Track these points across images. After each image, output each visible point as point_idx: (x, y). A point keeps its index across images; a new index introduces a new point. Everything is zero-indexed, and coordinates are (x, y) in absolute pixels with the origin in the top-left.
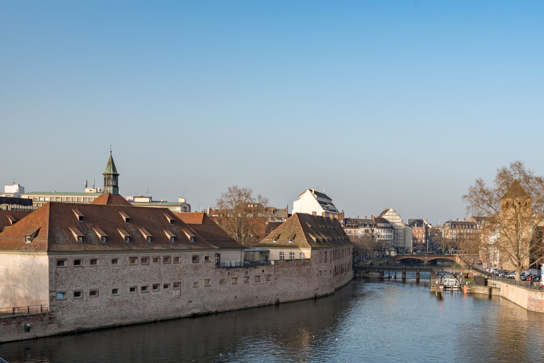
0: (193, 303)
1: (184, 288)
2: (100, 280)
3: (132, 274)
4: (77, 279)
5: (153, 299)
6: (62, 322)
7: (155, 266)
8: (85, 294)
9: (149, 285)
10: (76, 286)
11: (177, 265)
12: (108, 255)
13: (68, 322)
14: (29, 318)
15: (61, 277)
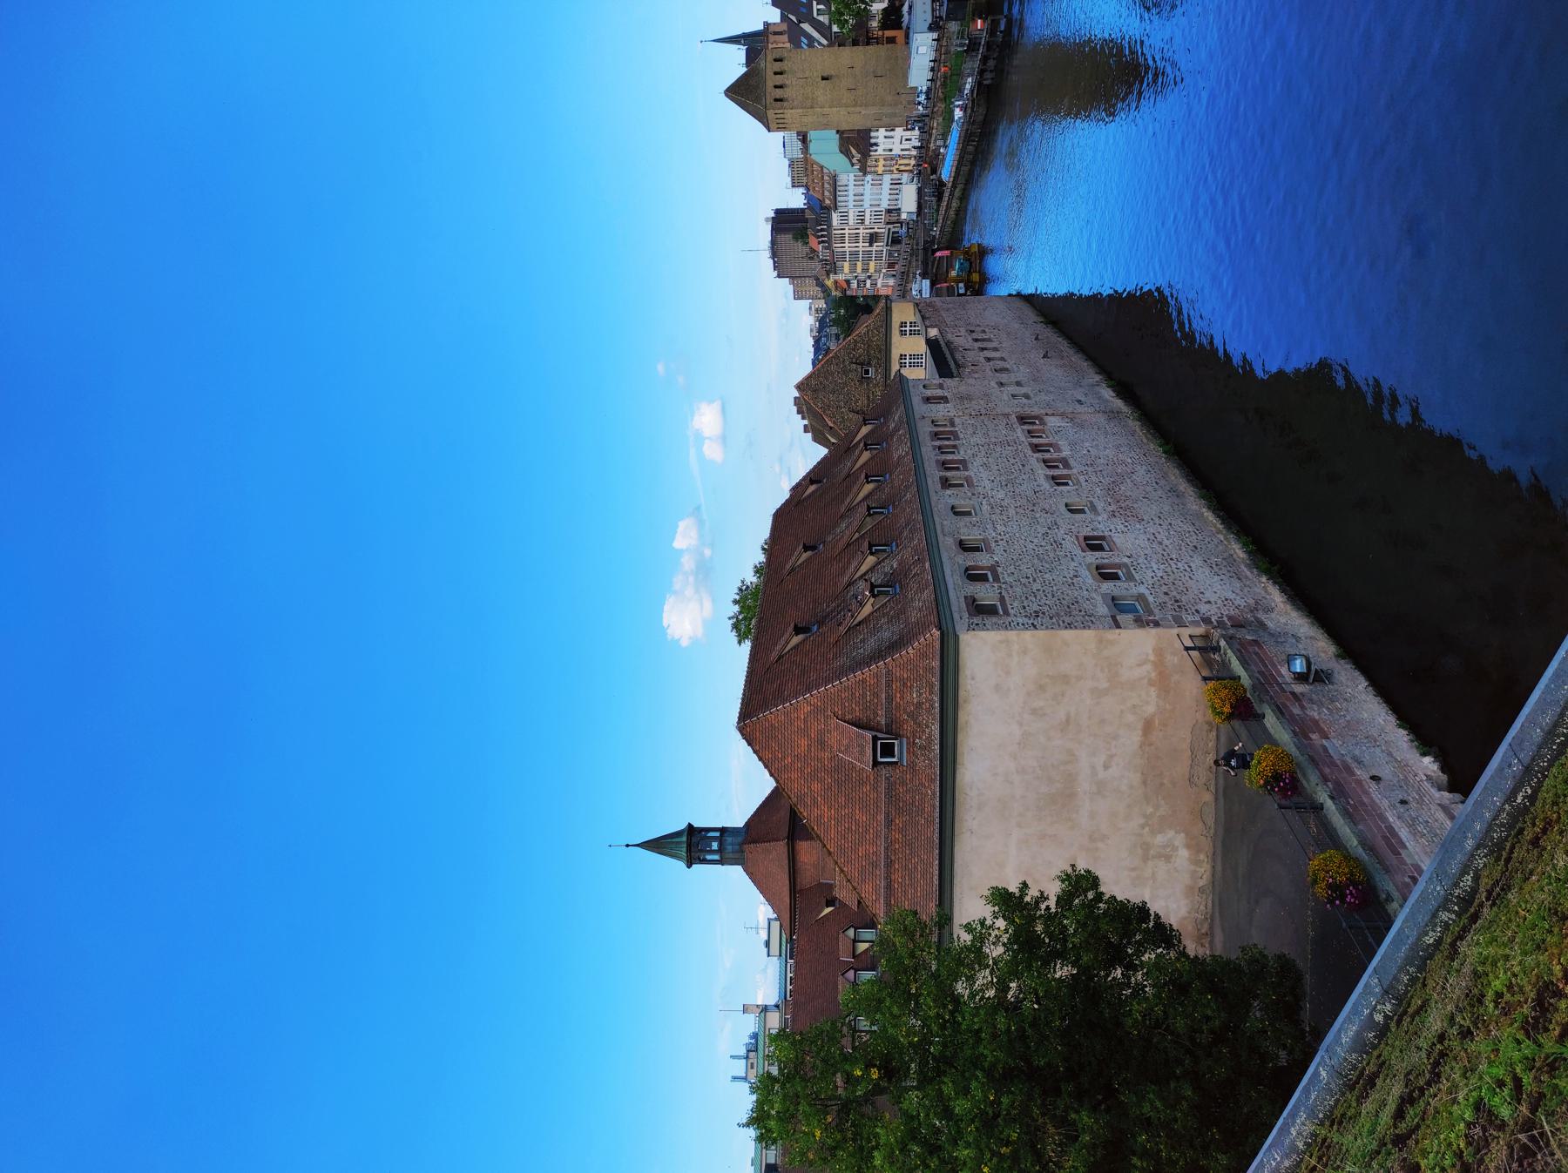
0: (1083, 399)
1: (1036, 411)
2: (1039, 535)
3: (1004, 483)
4: (1046, 576)
7: (969, 451)
8: (1106, 561)
9: (1037, 459)
10: (1076, 576)
11: (957, 421)
12: (942, 525)
13: (1238, 591)
14: (1260, 672)
15: (1047, 608)
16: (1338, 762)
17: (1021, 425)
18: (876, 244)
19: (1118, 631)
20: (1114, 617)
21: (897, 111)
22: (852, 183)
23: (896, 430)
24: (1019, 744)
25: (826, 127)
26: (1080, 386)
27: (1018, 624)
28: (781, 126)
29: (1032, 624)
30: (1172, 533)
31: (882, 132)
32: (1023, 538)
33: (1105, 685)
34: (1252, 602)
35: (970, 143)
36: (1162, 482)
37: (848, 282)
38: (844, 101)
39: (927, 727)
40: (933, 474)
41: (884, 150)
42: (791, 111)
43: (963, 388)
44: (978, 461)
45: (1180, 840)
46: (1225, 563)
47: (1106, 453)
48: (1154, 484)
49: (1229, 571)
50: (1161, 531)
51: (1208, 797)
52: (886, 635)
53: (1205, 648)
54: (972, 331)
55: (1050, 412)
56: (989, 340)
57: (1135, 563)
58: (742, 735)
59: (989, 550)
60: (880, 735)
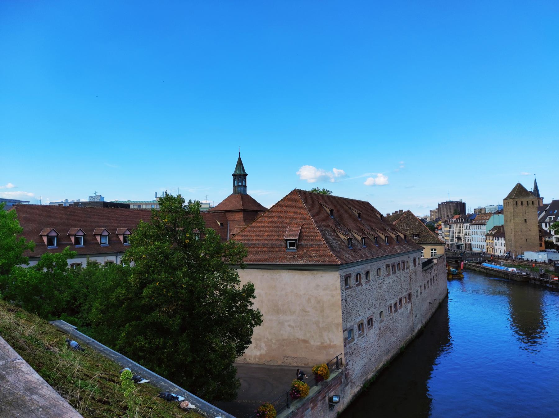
0: (417, 317)
1: (413, 300)
3: (388, 288)
5: (400, 319)
6: (353, 378)
9: (397, 300)
10: (359, 315)
13: (357, 376)
16: (304, 414)
17: (408, 294)
18: (457, 240)
19: (342, 331)
20: (346, 330)
21: (513, 247)
22: (482, 231)
23: (404, 247)
24: (297, 294)
25: (506, 221)
26: (421, 316)
27: (343, 294)
28: (506, 204)
29: (343, 299)
30: (375, 351)
31: (504, 242)
32: (371, 295)
33: (321, 326)
34: (354, 381)
35: (504, 275)
36: (391, 347)
37: (441, 229)
38: (516, 227)
39: (302, 259)
40: (390, 261)
41: (496, 243)
42: (512, 208)
43: (419, 272)
44: (395, 278)
45: (263, 352)
46: (366, 371)
47: (400, 326)
48: (390, 344)
49: (363, 372)
50: (375, 347)
51: (280, 363)
52: (335, 244)
53: (338, 364)
54: (436, 276)
55: (413, 305)
56: (434, 282)
57: (364, 337)
58: (293, 191)
59: (367, 282)
60: (297, 242)
